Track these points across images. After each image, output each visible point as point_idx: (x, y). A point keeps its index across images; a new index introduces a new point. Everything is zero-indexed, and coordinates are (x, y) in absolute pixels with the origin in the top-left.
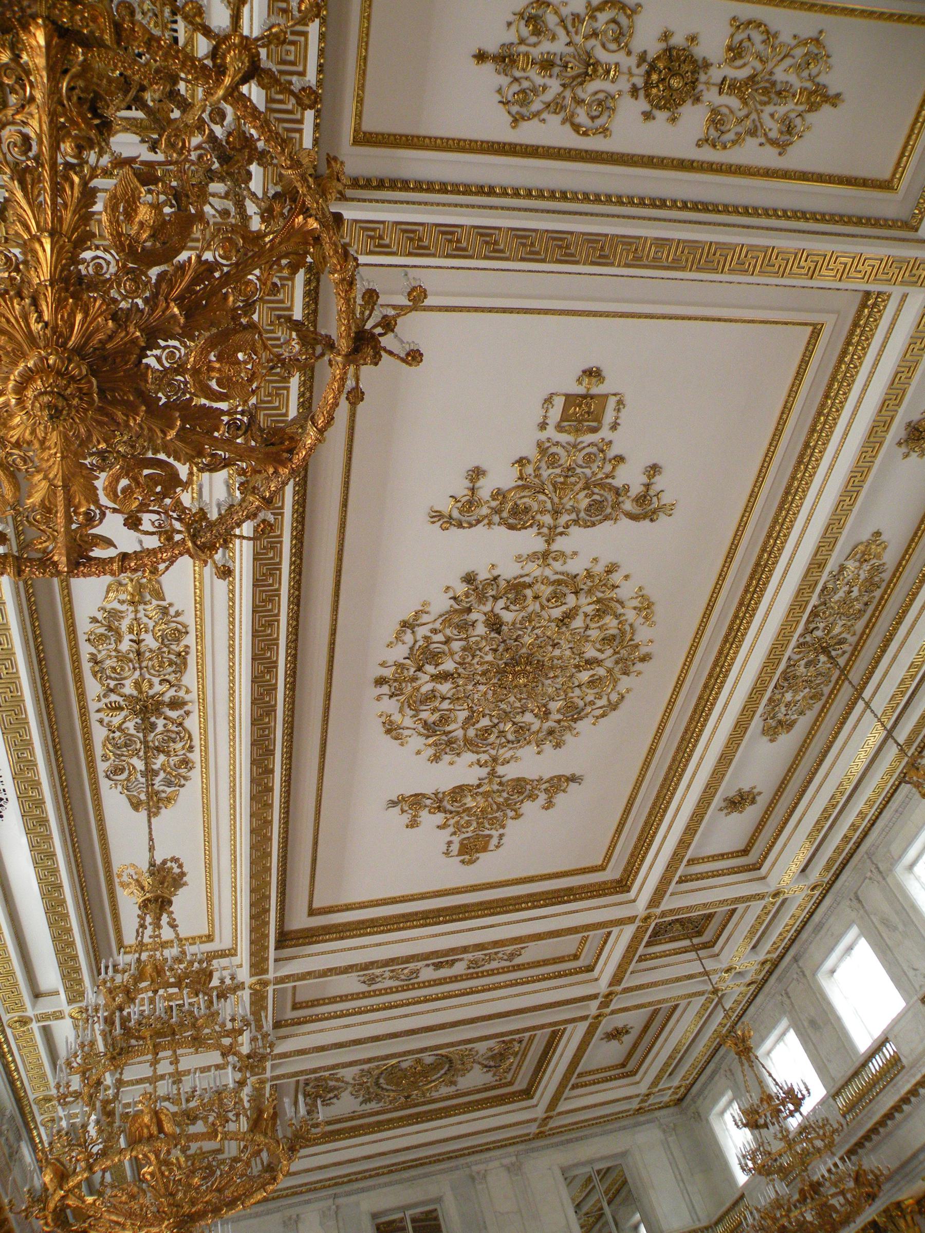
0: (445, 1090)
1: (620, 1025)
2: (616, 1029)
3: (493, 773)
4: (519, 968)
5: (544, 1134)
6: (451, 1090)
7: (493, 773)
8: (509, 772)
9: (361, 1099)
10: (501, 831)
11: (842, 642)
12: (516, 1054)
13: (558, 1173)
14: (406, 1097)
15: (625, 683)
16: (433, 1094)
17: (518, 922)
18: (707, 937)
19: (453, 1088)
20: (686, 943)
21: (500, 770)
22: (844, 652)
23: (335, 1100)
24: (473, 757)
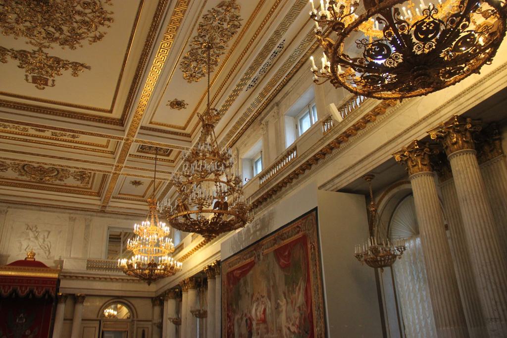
0: (58, 182)
1: (138, 180)
2: (135, 181)
3: (40, 50)
4: (77, 142)
5: (103, 211)
6: (62, 183)
7: (40, 50)
8: (51, 53)
9: (18, 173)
10: (52, 78)
11: (222, 48)
13: (106, 229)
15: (101, 29)
17: (51, 120)
18: (171, 157)
20: (154, 156)
21: (45, 50)
22: (223, 53)
23: (5, 170)
24: (28, 40)
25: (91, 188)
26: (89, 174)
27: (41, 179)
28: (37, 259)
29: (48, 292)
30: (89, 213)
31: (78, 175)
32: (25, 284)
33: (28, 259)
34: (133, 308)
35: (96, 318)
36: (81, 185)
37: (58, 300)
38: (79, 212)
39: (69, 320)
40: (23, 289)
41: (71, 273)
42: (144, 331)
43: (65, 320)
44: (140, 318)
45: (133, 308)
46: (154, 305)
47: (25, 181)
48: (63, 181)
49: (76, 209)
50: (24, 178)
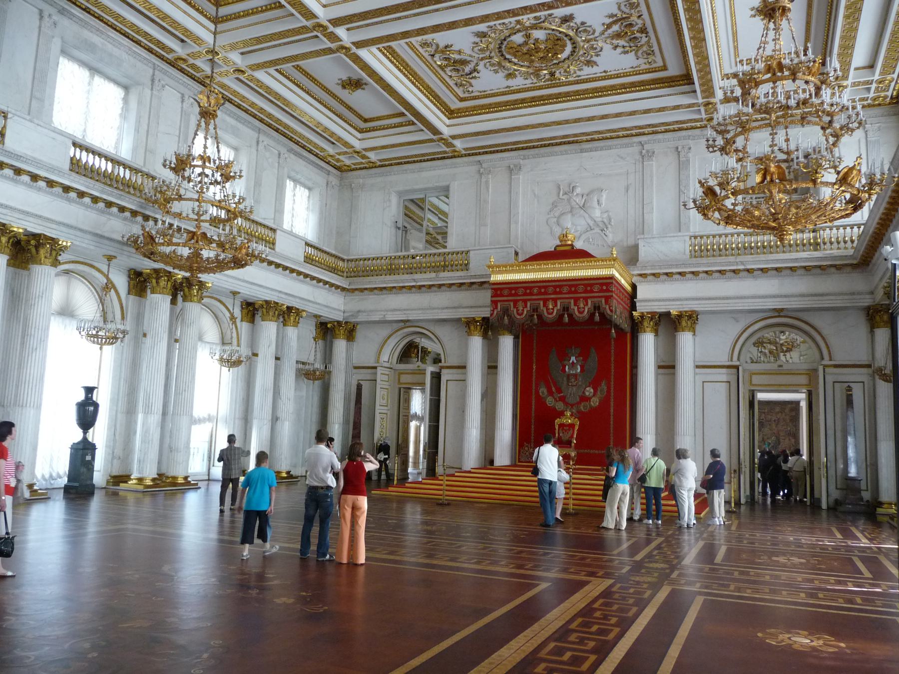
0: (587, 71)
12: (643, 30)
14: (552, 74)
16: (579, 73)
19: (595, 69)
25: (665, 68)
26: (640, 22)
27: (552, 74)
28: (579, 245)
29: (599, 307)
30: (684, 133)
31: (618, 36)
32: (553, 296)
33: (558, 249)
34: (818, 338)
35: (730, 363)
36: (642, 64)
37: (636, 327)
38: (660, 136)
39: (668, 367)
40: (551, 307)
41: (653, 267)
42: (849, 389)
43: (660, 367)
44: (839, 359)
45: (818, 338)
46: (873, 325)
47: (519, 91)
48: (595, 63)
49: (654, 130)
50: (518, 82)
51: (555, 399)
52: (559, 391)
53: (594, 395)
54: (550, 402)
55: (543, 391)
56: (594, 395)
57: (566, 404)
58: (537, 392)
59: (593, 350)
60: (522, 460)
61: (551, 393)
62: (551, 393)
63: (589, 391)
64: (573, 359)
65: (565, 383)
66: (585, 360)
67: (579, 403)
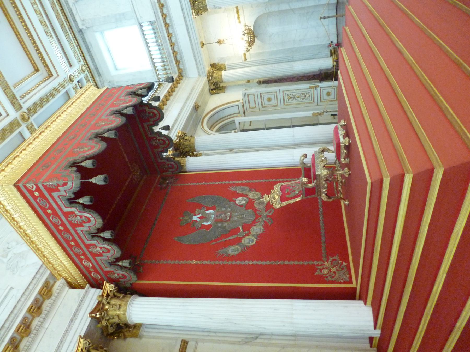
34: (224, 107)
51: (246, 235)
52: (236, 231)
53: (246, 196)
54: (249, 241)
55: (232, 250)
56: (246, 196)
57: (254, 223)
58: (233, 258)
59: (190, 200)
60: (346, 278)
61: (238, 241)
62: (238, 241)
63: (240, 201)
64: (195, 218)
65: (225, 224)
66: (200, 206)
67: (255, 210)
